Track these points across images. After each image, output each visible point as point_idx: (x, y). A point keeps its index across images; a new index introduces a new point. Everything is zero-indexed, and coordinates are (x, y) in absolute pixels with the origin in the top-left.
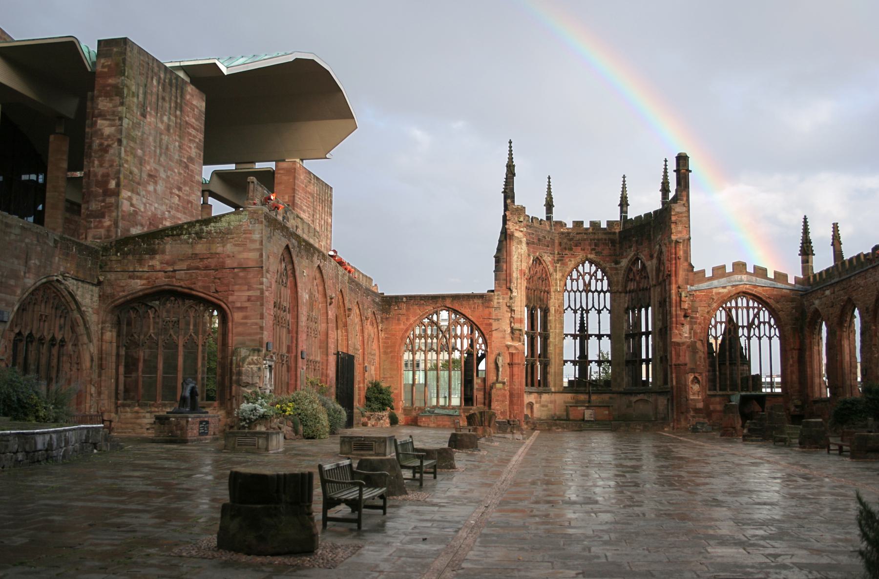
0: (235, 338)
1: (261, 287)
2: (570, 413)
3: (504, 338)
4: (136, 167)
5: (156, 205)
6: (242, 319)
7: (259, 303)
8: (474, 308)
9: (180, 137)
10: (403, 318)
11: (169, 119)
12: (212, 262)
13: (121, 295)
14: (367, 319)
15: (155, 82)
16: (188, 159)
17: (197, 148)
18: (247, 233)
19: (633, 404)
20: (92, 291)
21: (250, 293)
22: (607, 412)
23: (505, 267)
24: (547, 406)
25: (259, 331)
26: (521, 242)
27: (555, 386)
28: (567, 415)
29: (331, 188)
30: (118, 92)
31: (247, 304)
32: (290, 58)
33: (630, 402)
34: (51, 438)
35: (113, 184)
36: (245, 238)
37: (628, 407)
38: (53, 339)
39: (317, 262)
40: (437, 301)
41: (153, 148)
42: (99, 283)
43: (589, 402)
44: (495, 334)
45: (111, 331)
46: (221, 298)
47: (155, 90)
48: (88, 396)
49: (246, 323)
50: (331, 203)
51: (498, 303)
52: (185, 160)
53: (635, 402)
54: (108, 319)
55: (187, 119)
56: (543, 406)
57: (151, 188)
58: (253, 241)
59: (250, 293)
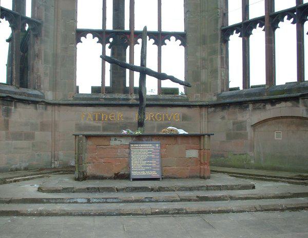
2: (87, 156)
19: (249, 129)
22: (193, 154)
24: (29, 137)
27: (54, 87)
28: (79, 160)
33: (240, 126)
37: (230, 137)
43: (141, 124)
53: (254, 126)
56: (18, 136)
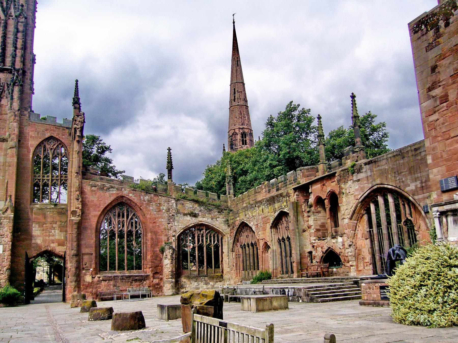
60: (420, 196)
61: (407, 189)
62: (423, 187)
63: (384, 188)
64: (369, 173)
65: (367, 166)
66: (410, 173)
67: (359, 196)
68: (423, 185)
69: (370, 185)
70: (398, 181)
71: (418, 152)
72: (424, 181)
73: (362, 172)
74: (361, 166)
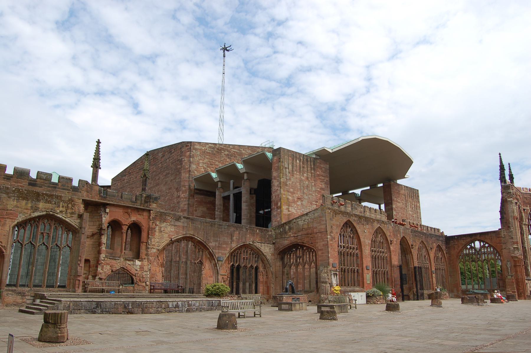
0: (319, 262)
1: (327, 240)
3: (510, 252)
4: (290, 196)
5: (303, 210)
6: (322, 254)
7: (327, 247)
8: (491, 238)
9: (315, 181)
10: (456, 246)
11: (307, 175)
12: (310, 231)
13: (281, 248)
14: (431, 248)
15: (298, 161)
16: (320, 189)
17: (325, 184)
18: (321, 218)
20: (270, 246)
21: (323, 243)
23: (505, 216)
25: (328, 258)
26: (512, 202)
29: (418, 190)
30: (278, 168)
31: (323, 248)
32: (360, 139)
34: (177, 303)
35: (279, 204)
36: (320, 220)
38: (252, 266)
39: (376, 225)
40: (473, 237)
41: (299, 188)
42: (274, 244)
44: (504, 251)
45: (280, 262)
46: (313, 246)
47: (298, 165)
48: (271, 288)
49: (323, 256)
50: (418, 196)
51: (504, 235)
52: (319, 190)
54: (278, 257)
55: (318, 173)
57: (299, 203)
58: (323, 221)
59: (323, 243)
60: (217, 251)
61: (210, 244)
62: (219, 246)
63: (195, 238)
64: (186, 225)
65: (185, 219)
66: (214, 237)
67: (173, 237)
68: (220, 245)
69: (185, 233)
70: (205, 238)
71: (221, 227)
72: (220, 243)
73: (180, 221)
74: (180, 217)
